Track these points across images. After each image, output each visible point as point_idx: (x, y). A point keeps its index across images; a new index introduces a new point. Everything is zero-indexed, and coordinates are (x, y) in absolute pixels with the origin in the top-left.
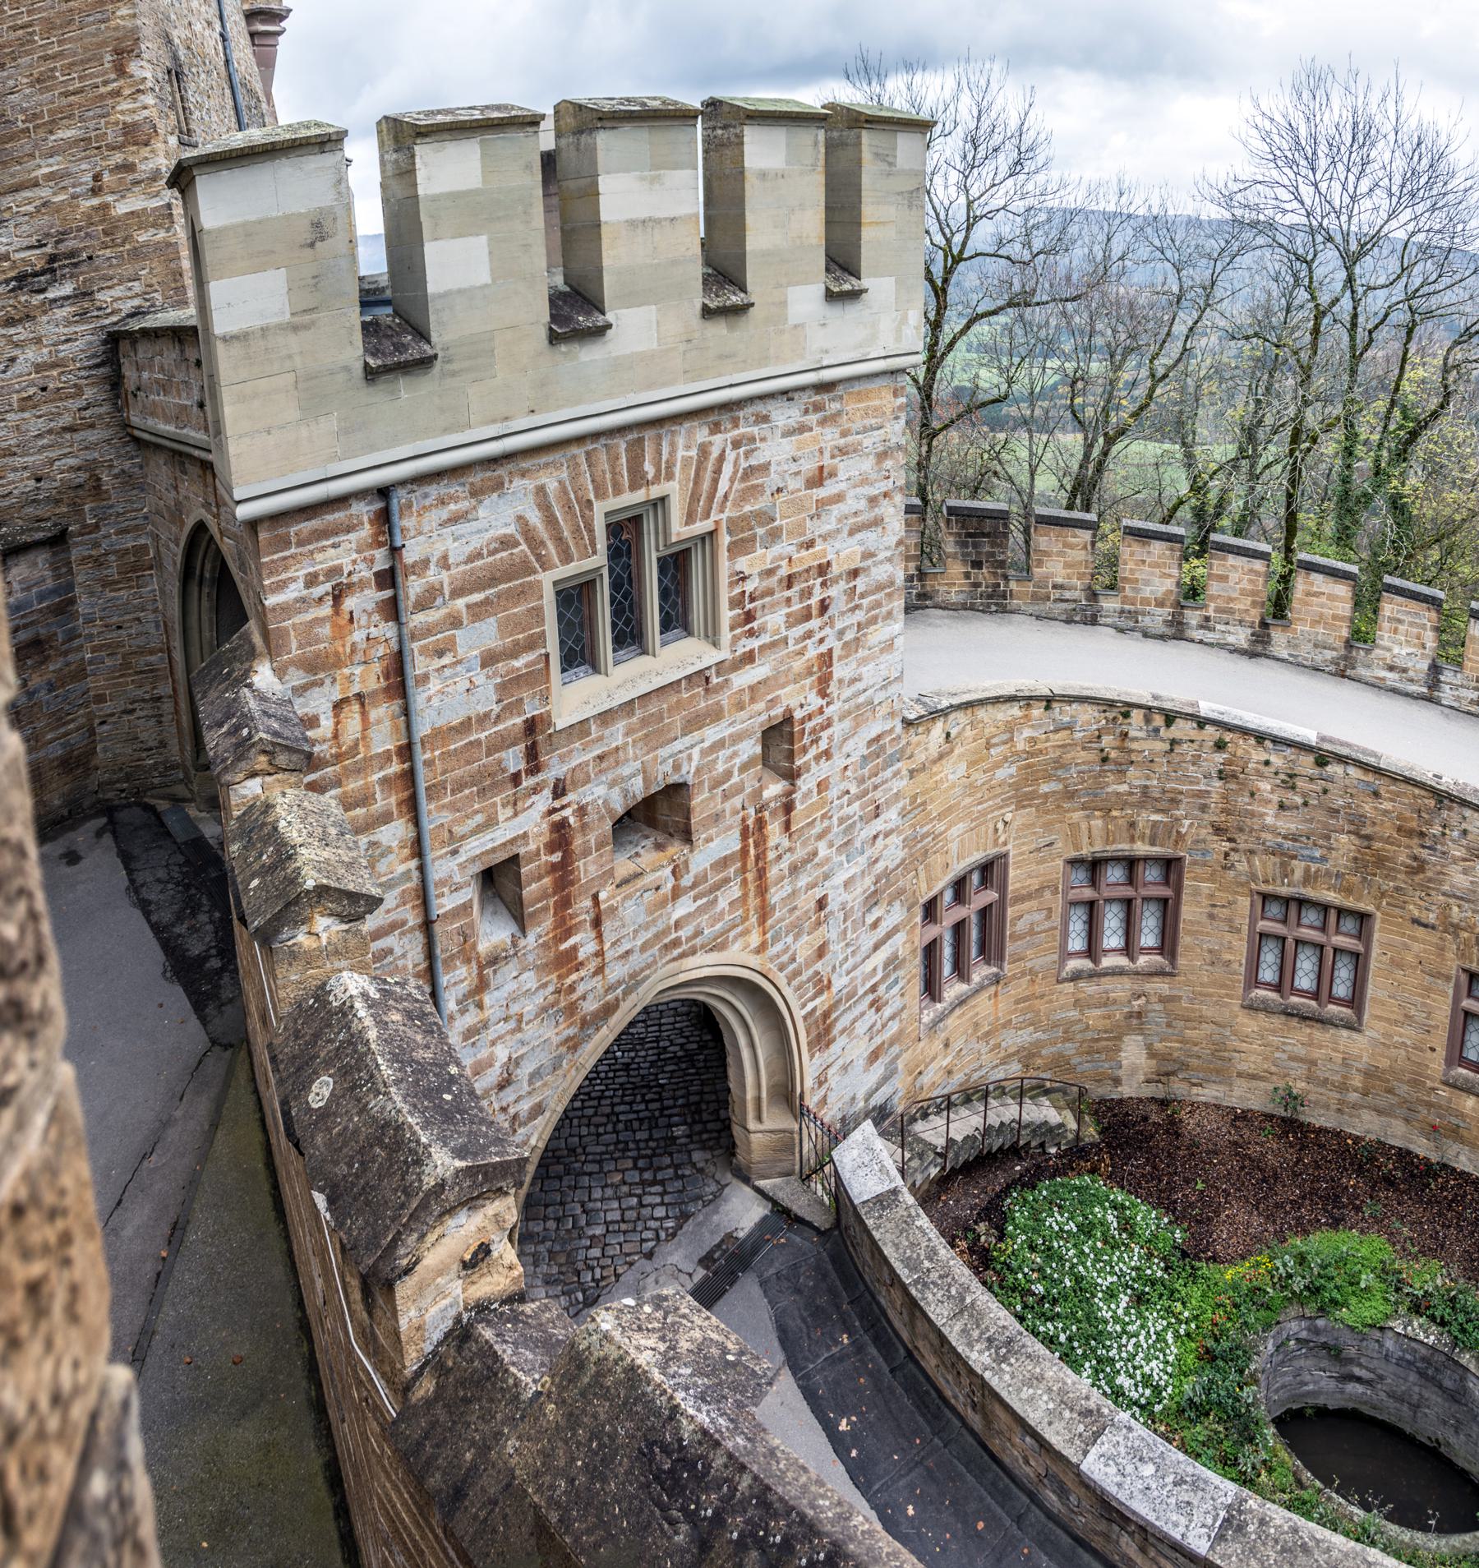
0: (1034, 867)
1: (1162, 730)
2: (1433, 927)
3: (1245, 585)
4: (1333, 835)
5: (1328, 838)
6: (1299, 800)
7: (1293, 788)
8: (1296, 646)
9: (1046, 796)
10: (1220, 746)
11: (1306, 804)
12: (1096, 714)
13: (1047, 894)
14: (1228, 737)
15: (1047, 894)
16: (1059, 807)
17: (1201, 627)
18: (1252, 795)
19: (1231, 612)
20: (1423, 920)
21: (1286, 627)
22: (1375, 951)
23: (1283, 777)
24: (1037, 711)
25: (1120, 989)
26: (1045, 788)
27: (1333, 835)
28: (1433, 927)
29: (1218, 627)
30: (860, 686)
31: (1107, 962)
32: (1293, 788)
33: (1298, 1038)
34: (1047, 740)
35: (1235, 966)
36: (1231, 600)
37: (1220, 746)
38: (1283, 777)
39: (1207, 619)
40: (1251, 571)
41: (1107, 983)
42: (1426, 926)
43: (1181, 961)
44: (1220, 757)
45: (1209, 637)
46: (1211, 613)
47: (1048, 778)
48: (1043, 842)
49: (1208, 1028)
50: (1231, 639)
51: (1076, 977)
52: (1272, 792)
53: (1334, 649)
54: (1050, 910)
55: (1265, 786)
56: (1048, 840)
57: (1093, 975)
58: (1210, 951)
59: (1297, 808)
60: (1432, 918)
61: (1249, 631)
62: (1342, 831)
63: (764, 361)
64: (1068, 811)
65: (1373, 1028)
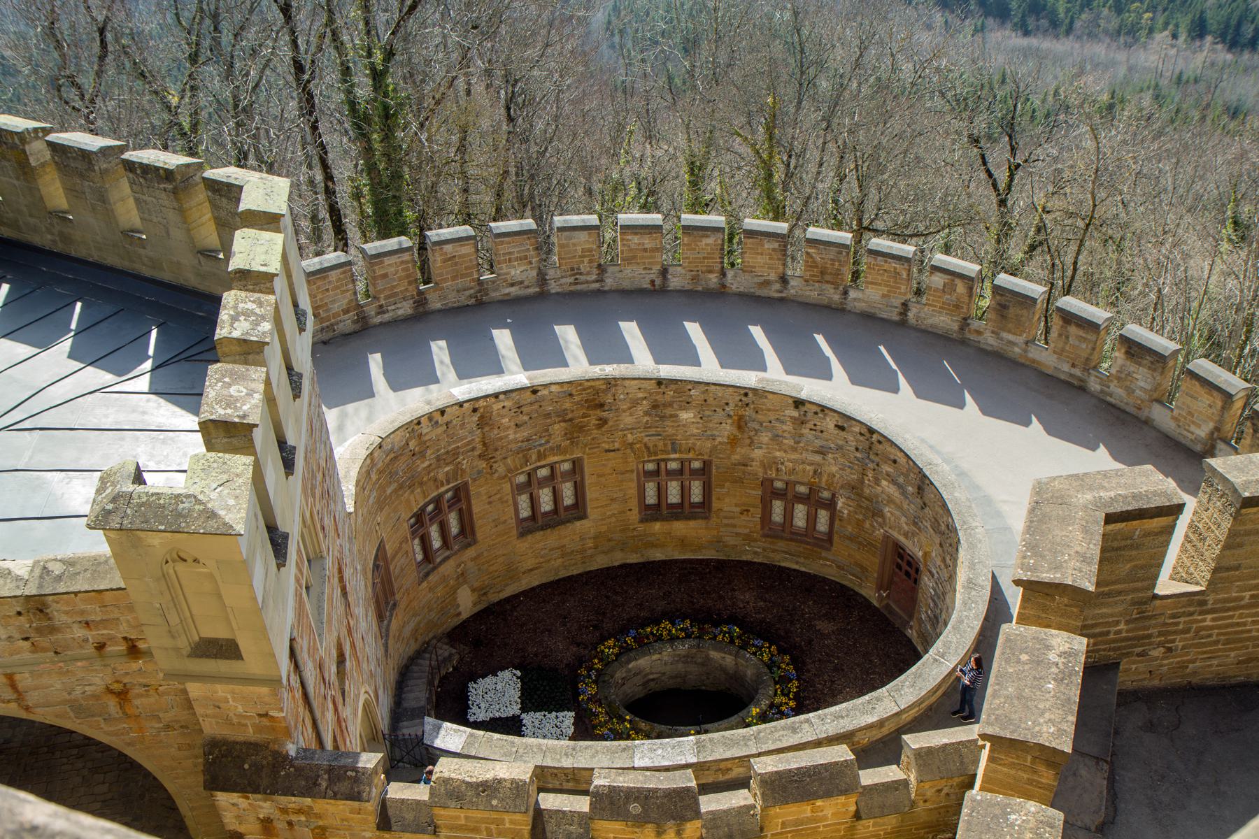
3: (401, 274)
8: (445, 298)
17: (379, 313)
19: (396, 294)
29: (389, 308)
35: (510, 521)
36: (394, 287)
39: (381, 306)
40: (402, 262)
41: (442, 569)
45: (386, 317)
46: (383, 302)
50: (400, 312)
53: (471, 288)
58: (494, 521)
61: (411, 302)
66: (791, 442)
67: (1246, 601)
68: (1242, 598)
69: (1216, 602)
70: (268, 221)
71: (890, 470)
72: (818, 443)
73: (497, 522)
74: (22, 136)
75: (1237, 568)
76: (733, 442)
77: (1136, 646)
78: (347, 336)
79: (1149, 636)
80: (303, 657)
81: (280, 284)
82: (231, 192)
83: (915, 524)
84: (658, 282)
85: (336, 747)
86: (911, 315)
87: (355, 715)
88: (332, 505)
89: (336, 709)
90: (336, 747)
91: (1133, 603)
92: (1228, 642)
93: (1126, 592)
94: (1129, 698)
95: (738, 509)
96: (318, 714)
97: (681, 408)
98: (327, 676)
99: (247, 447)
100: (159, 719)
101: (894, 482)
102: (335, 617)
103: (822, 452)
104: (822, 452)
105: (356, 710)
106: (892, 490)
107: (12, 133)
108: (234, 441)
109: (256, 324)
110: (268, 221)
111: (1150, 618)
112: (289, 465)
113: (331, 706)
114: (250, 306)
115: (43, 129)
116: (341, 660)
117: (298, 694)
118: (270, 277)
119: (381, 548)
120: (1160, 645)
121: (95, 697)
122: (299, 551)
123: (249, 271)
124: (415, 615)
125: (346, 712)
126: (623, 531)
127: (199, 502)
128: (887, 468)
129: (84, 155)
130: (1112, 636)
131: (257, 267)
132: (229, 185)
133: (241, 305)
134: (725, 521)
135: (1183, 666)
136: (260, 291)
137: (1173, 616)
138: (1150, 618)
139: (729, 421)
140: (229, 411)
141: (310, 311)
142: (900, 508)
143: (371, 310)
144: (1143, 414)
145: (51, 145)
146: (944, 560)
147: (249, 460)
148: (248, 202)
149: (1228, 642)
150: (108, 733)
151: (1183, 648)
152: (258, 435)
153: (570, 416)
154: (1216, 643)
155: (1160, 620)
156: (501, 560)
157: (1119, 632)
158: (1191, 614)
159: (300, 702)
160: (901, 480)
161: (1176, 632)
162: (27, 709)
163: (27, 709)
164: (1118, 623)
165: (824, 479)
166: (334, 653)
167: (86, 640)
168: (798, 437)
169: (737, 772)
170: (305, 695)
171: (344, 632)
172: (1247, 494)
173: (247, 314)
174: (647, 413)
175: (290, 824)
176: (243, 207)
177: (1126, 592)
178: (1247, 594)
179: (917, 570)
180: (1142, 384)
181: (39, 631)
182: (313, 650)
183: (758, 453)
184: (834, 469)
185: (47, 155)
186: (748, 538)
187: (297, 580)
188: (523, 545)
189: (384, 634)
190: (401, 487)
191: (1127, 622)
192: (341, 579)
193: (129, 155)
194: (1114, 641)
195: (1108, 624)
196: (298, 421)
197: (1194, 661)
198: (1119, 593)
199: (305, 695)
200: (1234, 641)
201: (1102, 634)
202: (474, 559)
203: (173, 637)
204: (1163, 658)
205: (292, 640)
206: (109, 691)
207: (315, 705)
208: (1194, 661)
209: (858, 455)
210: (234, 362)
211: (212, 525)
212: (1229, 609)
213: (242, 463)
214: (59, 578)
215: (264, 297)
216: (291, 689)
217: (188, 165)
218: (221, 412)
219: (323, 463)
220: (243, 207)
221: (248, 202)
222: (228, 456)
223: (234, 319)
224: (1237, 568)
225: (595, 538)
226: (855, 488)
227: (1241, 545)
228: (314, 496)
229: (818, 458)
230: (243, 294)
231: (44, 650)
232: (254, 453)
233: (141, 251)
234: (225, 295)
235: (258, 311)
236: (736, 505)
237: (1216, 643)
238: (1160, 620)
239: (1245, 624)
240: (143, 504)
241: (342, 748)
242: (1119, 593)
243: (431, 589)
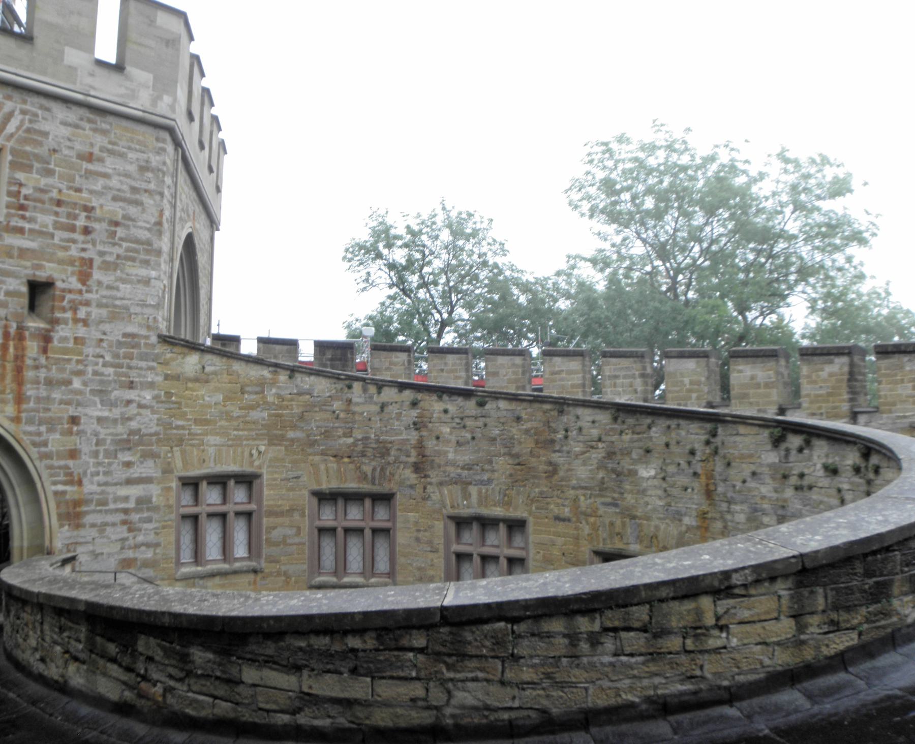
0: (284, 492)
1: (375, 396)
2: (569, 520)
4: (494, 459)
5: (490, 462)
6: (469, 436)
7: (464, 427)
9: (292, 441)
10: (414, 404)
11: (473, 438)
12: (328, 385)
13: (296, 516)
14: (420, 396)
15: (296, 516)
16: (303, 450)
18: (438, 438)
20: (562, 516)
23: (458, 420)
24: (283, 377)
26: (291, 434)
27: (494, 459)
28: (569, 520)
30: (114, 293)
32: (464, 427)
34: (292, 400)
37: (414, 404)
38: (458, 420)
42: (564, 520)
44: (414, 413)
47: (294, 427)
48: (291, 474)
52: (451, 433)
54: (299, 529)
55: (446, 430)
56: (295, 474)
59: (468, 443)
60: (566, 512)
62: (499, 455)
63: (44, 73)
64: (310, 455)
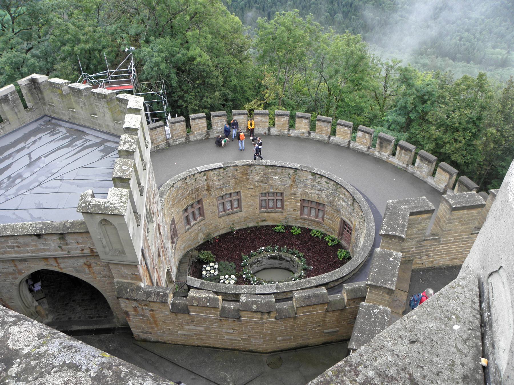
21: (192, 134)
22: (242, 197)
25: (195, 227)
31: (192, 224)
33: (230, 218)
43: (206, 216)
49: (213, 225)
51: (188, 229)
57: (191, 227)
65: (244, 210)
66: (311, 187)
67: (452, 241)
68: (451, 240)
69: (444, 241)
70: (136, 111)
71: (343, 197)
72: (319, 187)
73: (212, 212)
74: (62, 85)
75: (450, 230)
76: (291, 186)
77: (417, 255)
78: (162, 149)
79: (423, 252)
80: (147, 255)
81: (139, 132)
82: (125, 102)
83: (351, 215)
84: (267, 132)
85: (157, 285)
86: (351, 145)
87: (164, 274)
88: (156, 206)
89: (157, 273)
90: (157, 285)
91: (418, 242)
92: (447, 254)
93: (416, 238)
94: (415, 272)
95: (292, 209)
96: (152, 274)
97: (274, 175)
98: (154, 262)
99: (128, 186)
100: (101, 274)
101: (344, 201)
102: (157, 243)
103: (320, 190)
104: (320, 190)
105: (164, 273)
106: (344, 204)
107: (58, 84)
108: (124, 184)
109: (131, 146)
110: (136, 111)
111: (424, 246)
112: (142, 193)
113: (156, 271)
114: (130, 139)
115: (68, 83)
116: (159, 255)
117: (145, 268)
118: (136, 130)
119: (173, 220)
120: (426, 255)
121: (81, 266)
122: (145, 221)
123: (129, 128)
124: (184, 242)
125: (161, 274)
126: (254, 215)
127: (111, 204)
128: (341, 196)
129: (80, 90)
130: (411, 252)
131: (132, 127)
132: (124, 99)
133: (126, 139)
134: (289, 213)
135: (432, 261)
136: (133, 135)
137: (430, 246)
138: (424, 246)
139: (290, 180)
140: (122, 174)
141: (150, 141)
142: (346, 209)
143: (171, 141)
144: (425, 180)
145: (70, 87)
146: (360, 227)
147: (127, 190)
148: (130, 105)
149: (447, 254)
150: (86, 278)
151: (433, 256)
152: (131, 182)
153: (237, 177)
154: (443, 254)
155: (426, 247)
156: (213, 225)
157: (413, 251)
158: (436, 245)
159: (145, 270)
160: (346, 200)
161: (431, 251)
162: (61, 269)
163: (61, 269)
164: (413, 248)
165: (321, 199)
166: (157, 254)
167: (77, 248)
168: (313, 186)
169: (289, 295)
170: (147, 268)
171: (160, 248)
172: (454, 206)
173: (129, 142)
174: (262, 177)
175: (142, 309)
176: (128, 107)
177: (416, 238)
178: (453, 239)
179: (351, 230)
180: (425, 170)
181: (63, 245)
182: (150, 253)
183: (299, 190)
184: (324, 196)
185: (69, 90)
186: (295, 219)
187: (144, 230)
188: (221, 220)
189: (174, 249)
190: (180, 200)
191: (416, 248)
192: (159, 230)
193: (93, 90)
194: (412, 254)
195: (409, 248)
196: (145, 178)
197: (436, 260)
198: (413, 238)
199: (147, 268)
200: (448, 254)
201: (407, 252)
202: (204, 224)
203: (104, 248)
204: (427, 259)
205: (142, 250)
206: (85, 264)
207: (151, 271)
208: (436, 260)
209: (333, 192)
210: (124, 158)
211: (116, 212)
212: (447, 243)
213: (125, 191)
214: (69, 228)
215: (134, 137)
216: (142, 266)
217: (111, 93)
218: (119, 174)
219: (153, 192)
220: (128, 107)
221: (130, 105)
222: (121, 189)
223: (125, 143)
224: (450, 230)
225: (245, 218)
226: (331, 203)
227: (451, 223)
228: (150, 202)
229: (319, 192)
230: (127, 135)
231: (65, 251)
232: (130, 188)
233: (96, 121)
234: (122, 136)
235: (132, 141)
236: (292, 208)
237: (443, 254)
238: (426, 247)
239: (452, 248)
240: (94, 205)
241: (160, 285)
242: (413, 238)
243: (190, 234)
